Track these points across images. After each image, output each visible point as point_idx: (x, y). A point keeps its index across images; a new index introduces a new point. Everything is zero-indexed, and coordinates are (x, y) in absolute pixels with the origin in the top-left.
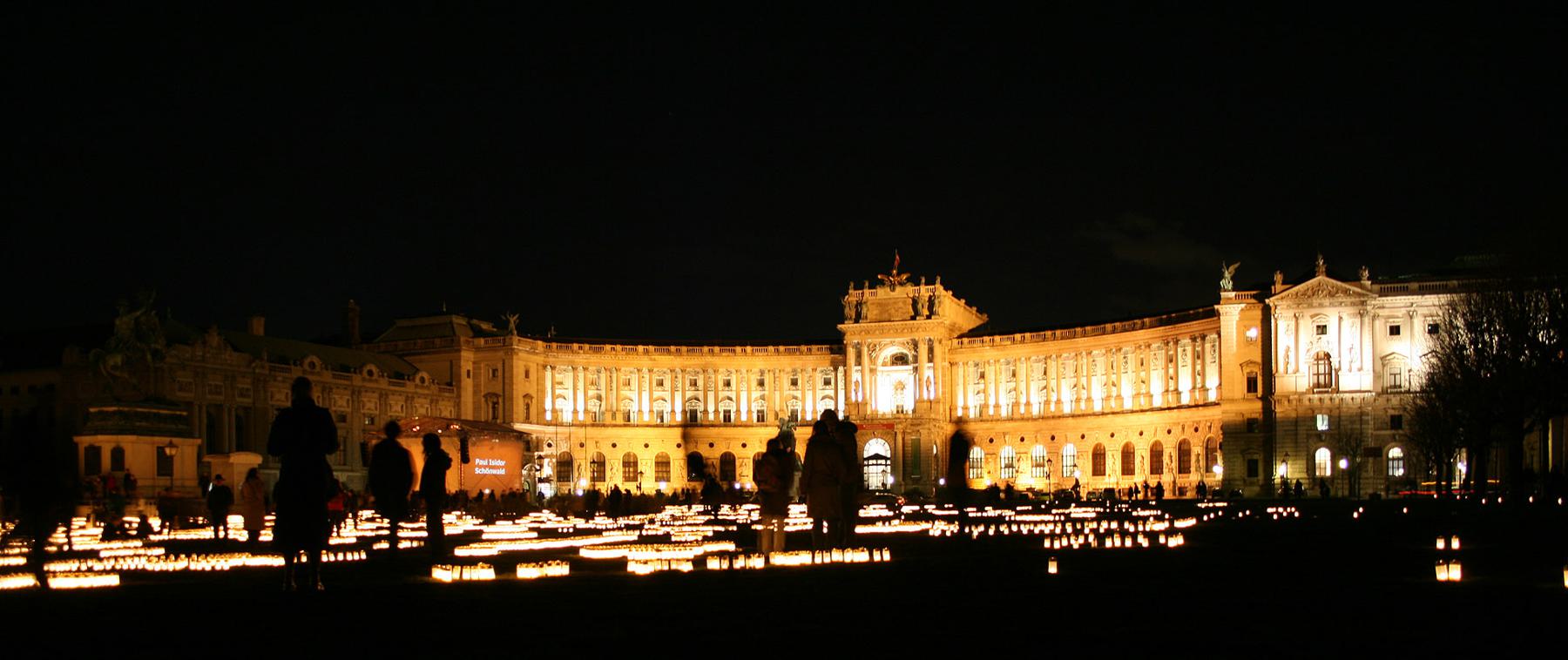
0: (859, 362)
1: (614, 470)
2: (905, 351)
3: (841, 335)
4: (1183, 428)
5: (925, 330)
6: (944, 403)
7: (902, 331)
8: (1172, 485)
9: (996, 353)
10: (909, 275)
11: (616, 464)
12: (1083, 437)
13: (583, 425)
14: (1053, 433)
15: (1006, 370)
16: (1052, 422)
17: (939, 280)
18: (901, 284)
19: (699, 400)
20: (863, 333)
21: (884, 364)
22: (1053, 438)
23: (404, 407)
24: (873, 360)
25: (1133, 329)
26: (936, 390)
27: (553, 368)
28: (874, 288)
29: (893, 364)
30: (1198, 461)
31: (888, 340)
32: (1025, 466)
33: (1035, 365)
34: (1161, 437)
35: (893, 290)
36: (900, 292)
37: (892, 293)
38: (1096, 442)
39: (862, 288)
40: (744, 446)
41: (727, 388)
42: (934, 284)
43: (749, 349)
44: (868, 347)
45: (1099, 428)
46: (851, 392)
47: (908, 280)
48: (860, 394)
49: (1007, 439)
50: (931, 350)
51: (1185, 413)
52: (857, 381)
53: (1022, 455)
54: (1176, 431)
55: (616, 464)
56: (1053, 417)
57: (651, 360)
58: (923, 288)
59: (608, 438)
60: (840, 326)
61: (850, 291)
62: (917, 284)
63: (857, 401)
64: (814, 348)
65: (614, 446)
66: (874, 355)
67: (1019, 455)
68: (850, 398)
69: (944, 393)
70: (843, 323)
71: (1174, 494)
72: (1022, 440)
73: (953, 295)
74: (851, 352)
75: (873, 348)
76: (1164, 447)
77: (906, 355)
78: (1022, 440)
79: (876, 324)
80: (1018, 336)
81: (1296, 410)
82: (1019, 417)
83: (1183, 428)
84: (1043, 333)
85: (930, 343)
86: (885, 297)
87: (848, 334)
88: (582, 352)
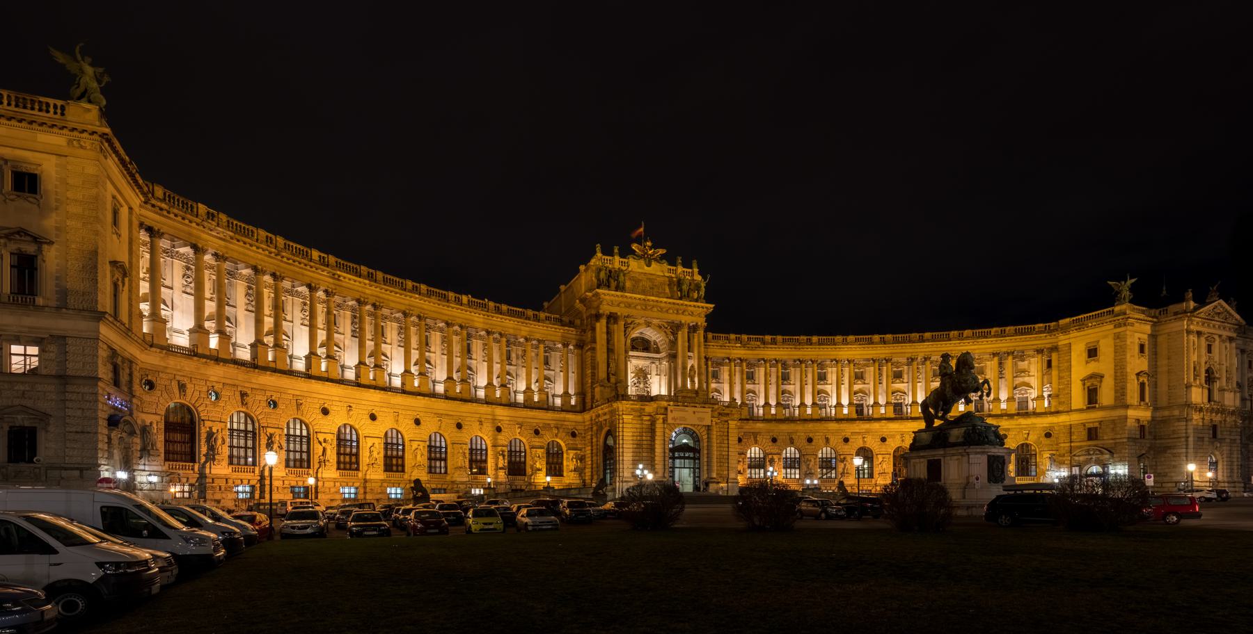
5: (692, 314)
7: (667, 311)
9: (743, 352)
10: (665, 251)
17: (695, 264)
18: (655, 260)
20: (622, 305)
31: (642, 321)
37: (646, 268)
39: (612, 255)
42: (691, 267)
47: (663, 257)
58: (680, 269)
61: (599, 254)
62: (672, 263)
80: (768, 338)
84: (796, 337)
86: (640, 271)
87: (604, 303)
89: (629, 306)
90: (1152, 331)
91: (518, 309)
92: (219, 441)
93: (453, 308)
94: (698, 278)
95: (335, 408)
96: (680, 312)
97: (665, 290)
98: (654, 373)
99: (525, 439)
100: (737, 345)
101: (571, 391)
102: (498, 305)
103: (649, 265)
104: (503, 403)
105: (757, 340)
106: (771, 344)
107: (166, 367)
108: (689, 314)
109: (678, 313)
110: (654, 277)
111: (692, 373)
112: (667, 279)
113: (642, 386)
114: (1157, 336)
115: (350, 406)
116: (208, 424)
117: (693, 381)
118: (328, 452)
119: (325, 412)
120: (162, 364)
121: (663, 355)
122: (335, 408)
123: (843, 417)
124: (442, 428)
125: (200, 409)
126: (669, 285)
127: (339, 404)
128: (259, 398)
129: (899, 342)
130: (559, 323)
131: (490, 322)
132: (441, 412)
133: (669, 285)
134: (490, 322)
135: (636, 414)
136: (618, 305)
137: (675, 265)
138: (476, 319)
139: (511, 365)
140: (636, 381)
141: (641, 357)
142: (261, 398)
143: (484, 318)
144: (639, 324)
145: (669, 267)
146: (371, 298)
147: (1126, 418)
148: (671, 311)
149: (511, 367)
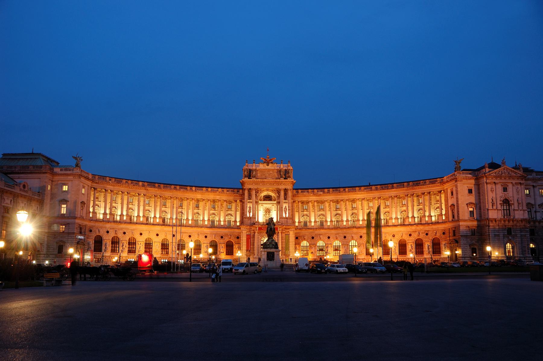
0: (250, 197)
1: (124, 247)
4: (419, 234)
9: (315, 197)
11: (125, 243)
12: (361, 237)
13: (108, 221)
14: (345, 235)
15: (317, 206)
16: (345, 230)
19: (166, 213)
22: (345, 237)
23: (12, 201)
25: (388, 189)
26: (289, 214)
27: (95, 189)
29: (264, 200)
30: (428, 249)
32: (331, 250)
34: (406, 238)
35: (268, 165)
37: (267, 166)
41: (180, 208)
46: (247, 212)
48: (251, 214)
49: (321, 237)
50: (286, 194)
51: (435, 227)
53: (329, 245)
55: (125, 243)
56: (345, 228)
57: (146, 189)
59: (122, 229)
65: (124, 233)
66: (258, 195)
67: (327, 245)
74: (246, 193)
75: (257, 191)
77: (271, 196)
78: (329, 238)
79: (262, 180)
81: (498, 225)
82: (327, 227)
83: (419, 234)
84: (339, 189)
85: (285, 191)
87: (246, 184)
88: (111, 182)
89: (257, 183)
90: (475, 182)
92: (108, 246)
94: (291, 168)
96: (280, 184)
98: (273, 210)
99: (217, 240)
100: (311, 195)
101: (238, 219)
103: (268, 165)
104: (208, 226)
105: (321, 191)
106: (327, 193)
107: (95, 226)
108: (283, 185)
111: (285, 209)
112: (276, 170)
113: (268, 216)
114: (479, 184)
115: (149, 232)
116: (105, 241)
117: (286, 213)
118: (141, 247)
119: (141, 234)
120: (95, 225)
121: (275, 202)
122: (144, 233)
123: (359, 226)
125: (103, 236)
126: (277, 172)
127: (145, 231)
128: (121, 231)
129: (383, 189)
133: (277, 172)
134: (204, 196)
135: (248, 230)
136: (252, 184)
139: (215, 210)
142: (122, 232)
144: (263, 190)
147: (459, 226)
148: (275, 184)
149: (215, 211)
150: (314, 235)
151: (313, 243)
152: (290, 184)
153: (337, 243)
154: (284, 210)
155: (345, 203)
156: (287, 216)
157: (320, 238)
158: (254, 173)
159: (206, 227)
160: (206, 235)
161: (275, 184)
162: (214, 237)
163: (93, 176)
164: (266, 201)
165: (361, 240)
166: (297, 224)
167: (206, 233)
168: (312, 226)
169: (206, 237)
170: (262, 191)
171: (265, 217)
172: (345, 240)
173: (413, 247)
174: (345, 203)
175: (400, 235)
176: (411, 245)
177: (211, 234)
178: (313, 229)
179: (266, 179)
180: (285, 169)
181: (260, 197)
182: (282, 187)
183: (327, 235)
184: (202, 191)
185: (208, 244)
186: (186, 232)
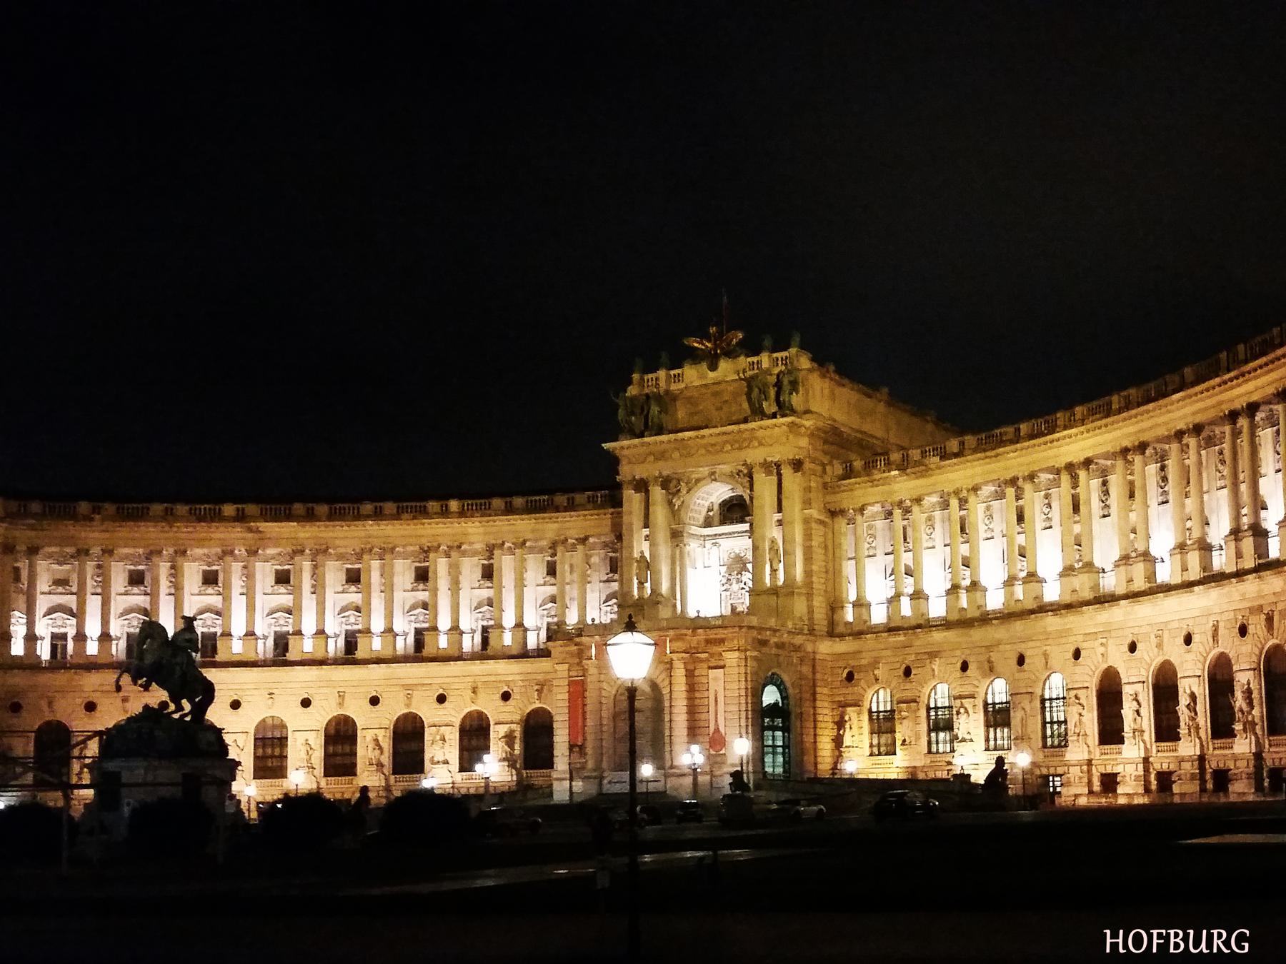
2: (739, 492)
3: (613, 461)
6: (809, 596)
8: (1252, 763)
10: (740, 336)
14: (1021, 648)
21: (708, 523)
22: (1021, 660)
24: (675, 513)
28: (680, 367)
31: (705, 471)
32: (971, 724)
33: (996, 504)
35: (713, 367)
36: (727, 369)
37: (711, 375)
38: (1105, 666)
39: (654, 370)
40: (441, 699)
41: (421, 586)
43: (454, 505)
44: (665, 483)
45: (1106, 633)
48: (648, 585)
52: (643, 557)
53: (963, 701)
54: (1257, 626)
58: (765, 360)
60: (606, 446)
61: (636, 376)
63: (641, 598)
64: (580, 498)
66: (677, 502)
68: (630, 591)
69: (808, 573)
70: (616, 440)
71: (1259, 788)
72: (965, 667)
73: (837, 371)
74: (632, 499)
76: (1235, 668)
78: (965, 667)
79: (672, 436)
84: (998, 431)
87: (624, 462)
89: (661, 456)
91: (542, 498)
93: (424, 524)
95: (250, 699)
97: (741, 405)
102: (508, 499)
104: (515, 652)
106: (956, 455)
108: (761, 444)
109: (740, 448)
110: (723, 386)
112: (744, 384)
117: (774, 571)
124: (414, 701)
130: (591, 505)
131: (494, 529)
132: (410, 682)
137: (757, 353)
138: (470, 530)
140: (724, 581)
141: (734, 533)
143: (482, 526)
145: (749, 359)
146: (305, 542)
148: (728, 447)
150: (913, 656)
151: (908, 695)
152: (784, 439)
153: (999, 691)
154: (767, 557)
155: (1043, 493)
156: (781, 582)
157: (933, 670)
158: (655, 409)
159: (474, 657)
160: (506, 689)
161: (728, 447)
162: (536, 697)
163: (19, 505)
164: (732, 523)
165: (1078, 670)
166: (849, 615)
167: (507, 683)
168: (903, 617)
169: (506, 697)
170: (693, 484)
171: (728, 593)
172: (1021, 675)
173: (1255, 695)
174: (1043, 493)
175: (1210, 634)
176: (1249, 683)
177: (527, 683)
178: (907, 629)
179: (706, 427)
180: (778, 375)
181: (709, 510)
182: (755, 455)
183: (958, 653)
184: (488, 512)
185: (514, 726)
186: (426, 681)
